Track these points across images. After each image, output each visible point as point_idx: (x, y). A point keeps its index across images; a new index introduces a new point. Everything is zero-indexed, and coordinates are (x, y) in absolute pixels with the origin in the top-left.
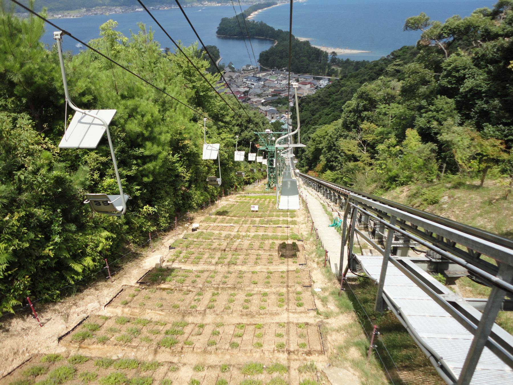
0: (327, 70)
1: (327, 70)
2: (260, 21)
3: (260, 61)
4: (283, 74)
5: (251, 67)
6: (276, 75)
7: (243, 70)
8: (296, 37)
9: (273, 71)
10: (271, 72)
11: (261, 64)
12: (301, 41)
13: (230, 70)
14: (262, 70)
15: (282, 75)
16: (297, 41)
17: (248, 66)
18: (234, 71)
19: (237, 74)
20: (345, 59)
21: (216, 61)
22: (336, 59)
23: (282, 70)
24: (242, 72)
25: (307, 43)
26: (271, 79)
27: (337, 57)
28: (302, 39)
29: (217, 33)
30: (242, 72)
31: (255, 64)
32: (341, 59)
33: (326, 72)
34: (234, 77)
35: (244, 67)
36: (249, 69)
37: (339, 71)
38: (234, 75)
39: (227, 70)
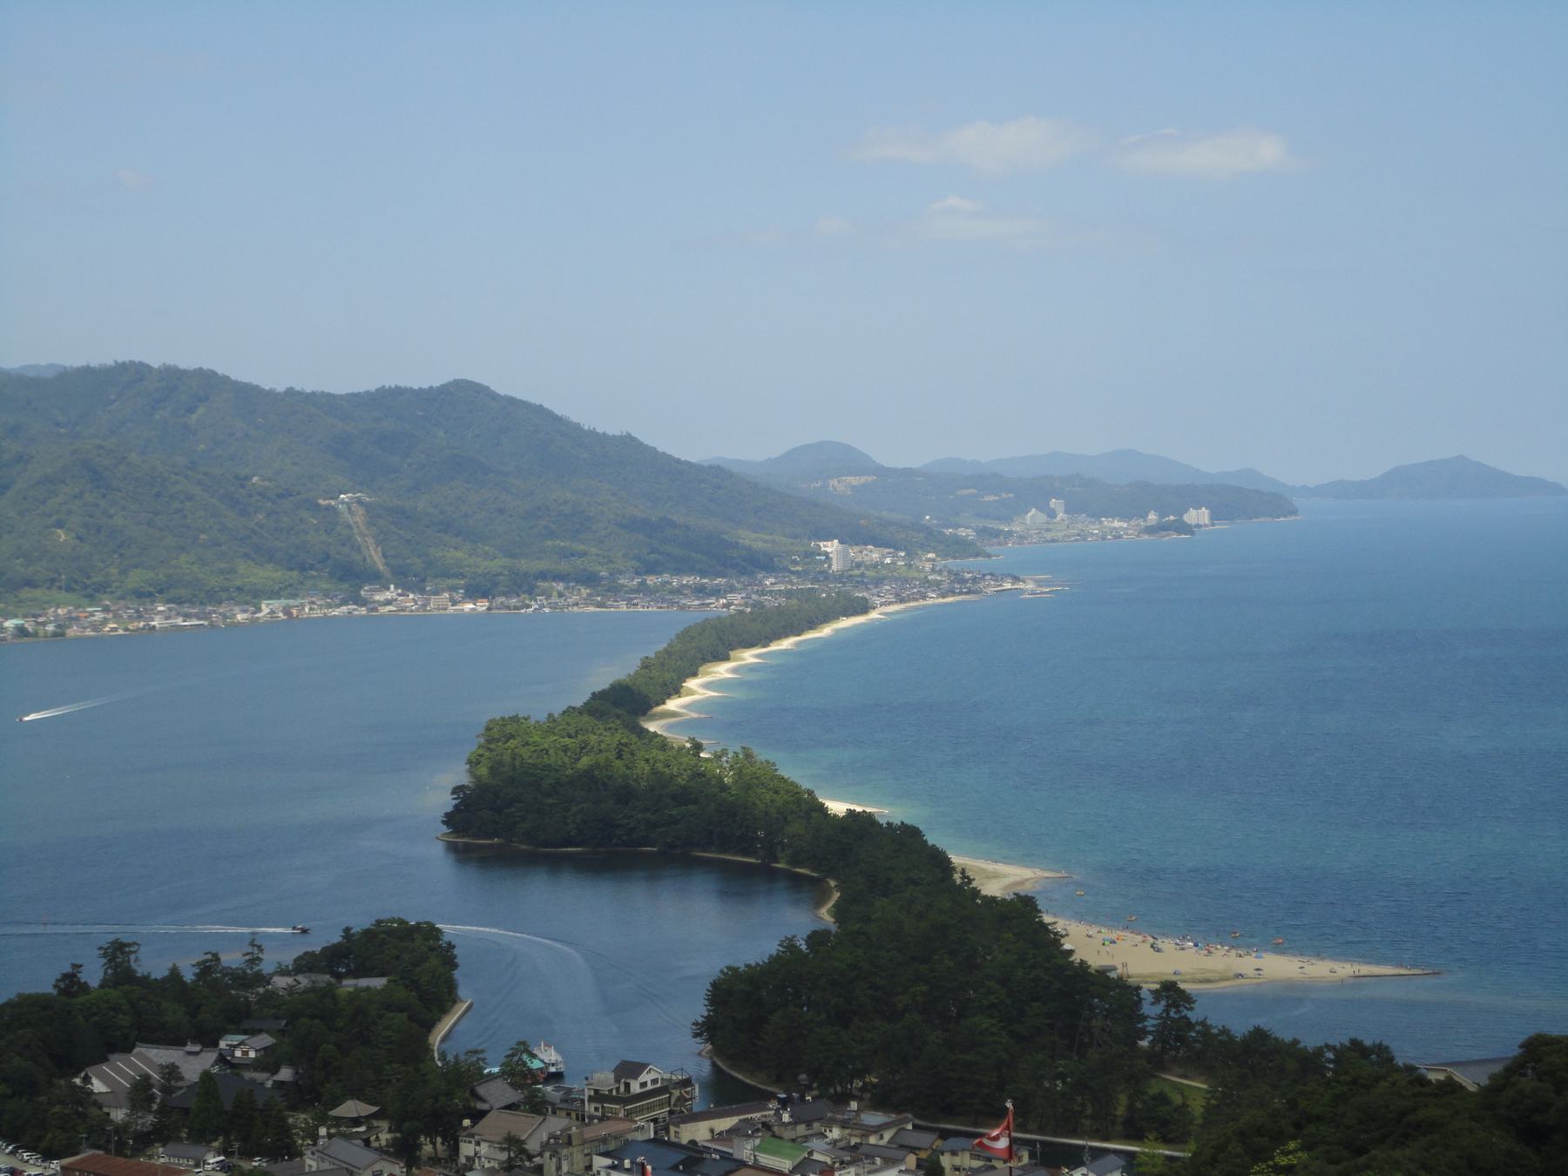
0: (1123, 1099)
1: (1123, 1099)
2: (734, 748)
3: (708, 1029)
4: (844, 1125)
5: (646, 1077)
6: (801, 1129)
7: (598, 1097)
8: (956, 860)
9: (784, 1104)
10: (768, 1112)
11: (718, 1051)
12: (992, 889)
13: (514, 1096)
14: (726, 1094)
15: (835, 1133)
16: (965, 893)
17: (629, 1069)
18: (537, 1106)
19: (556, 1124)
20: (1240, 1028)
21: (429, 1026)
22: (1190, 1025)
23: (842, 1100)
24: (590, 1108)
25: (1020, 914)
26: (766, 1160)
27: (1193, 1016)
28: (998, 877)
29: (449, 819)
30: (590, 1108)
31: (678, 1053)
32: (1216, 1021)
33: (1120, 1111)
34: (533, 1146)
35: (605, 1079)
36: (635, 1088)
37: (1197, 1107)
38: (536, 1133)
39: (497, 1093)
